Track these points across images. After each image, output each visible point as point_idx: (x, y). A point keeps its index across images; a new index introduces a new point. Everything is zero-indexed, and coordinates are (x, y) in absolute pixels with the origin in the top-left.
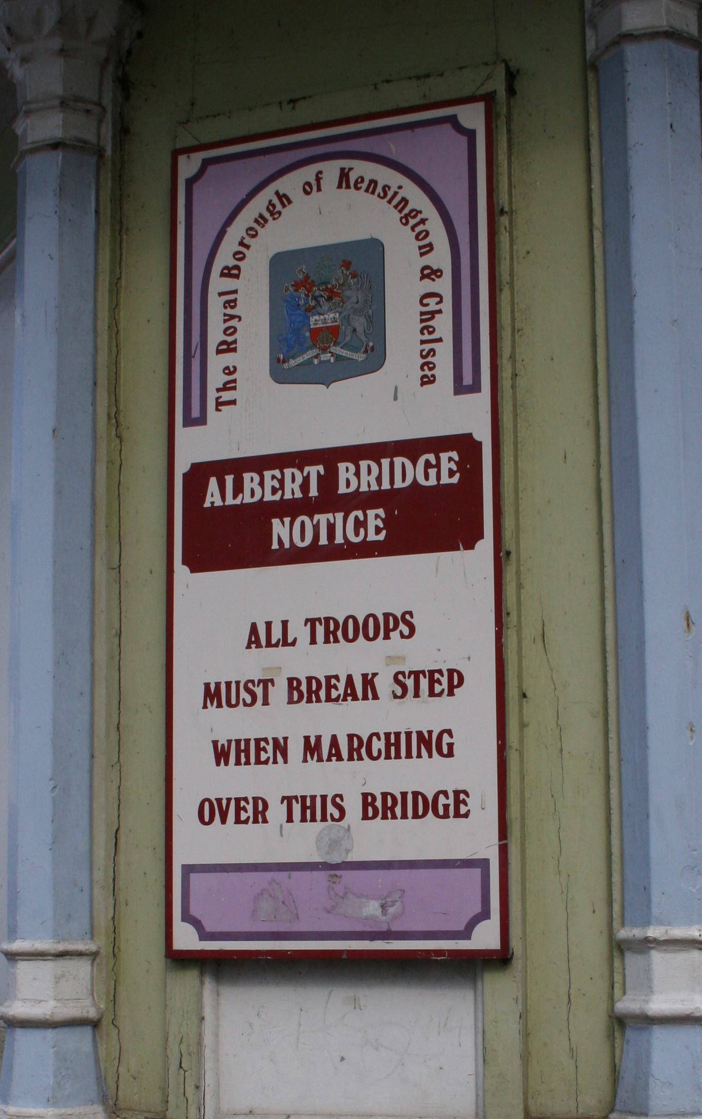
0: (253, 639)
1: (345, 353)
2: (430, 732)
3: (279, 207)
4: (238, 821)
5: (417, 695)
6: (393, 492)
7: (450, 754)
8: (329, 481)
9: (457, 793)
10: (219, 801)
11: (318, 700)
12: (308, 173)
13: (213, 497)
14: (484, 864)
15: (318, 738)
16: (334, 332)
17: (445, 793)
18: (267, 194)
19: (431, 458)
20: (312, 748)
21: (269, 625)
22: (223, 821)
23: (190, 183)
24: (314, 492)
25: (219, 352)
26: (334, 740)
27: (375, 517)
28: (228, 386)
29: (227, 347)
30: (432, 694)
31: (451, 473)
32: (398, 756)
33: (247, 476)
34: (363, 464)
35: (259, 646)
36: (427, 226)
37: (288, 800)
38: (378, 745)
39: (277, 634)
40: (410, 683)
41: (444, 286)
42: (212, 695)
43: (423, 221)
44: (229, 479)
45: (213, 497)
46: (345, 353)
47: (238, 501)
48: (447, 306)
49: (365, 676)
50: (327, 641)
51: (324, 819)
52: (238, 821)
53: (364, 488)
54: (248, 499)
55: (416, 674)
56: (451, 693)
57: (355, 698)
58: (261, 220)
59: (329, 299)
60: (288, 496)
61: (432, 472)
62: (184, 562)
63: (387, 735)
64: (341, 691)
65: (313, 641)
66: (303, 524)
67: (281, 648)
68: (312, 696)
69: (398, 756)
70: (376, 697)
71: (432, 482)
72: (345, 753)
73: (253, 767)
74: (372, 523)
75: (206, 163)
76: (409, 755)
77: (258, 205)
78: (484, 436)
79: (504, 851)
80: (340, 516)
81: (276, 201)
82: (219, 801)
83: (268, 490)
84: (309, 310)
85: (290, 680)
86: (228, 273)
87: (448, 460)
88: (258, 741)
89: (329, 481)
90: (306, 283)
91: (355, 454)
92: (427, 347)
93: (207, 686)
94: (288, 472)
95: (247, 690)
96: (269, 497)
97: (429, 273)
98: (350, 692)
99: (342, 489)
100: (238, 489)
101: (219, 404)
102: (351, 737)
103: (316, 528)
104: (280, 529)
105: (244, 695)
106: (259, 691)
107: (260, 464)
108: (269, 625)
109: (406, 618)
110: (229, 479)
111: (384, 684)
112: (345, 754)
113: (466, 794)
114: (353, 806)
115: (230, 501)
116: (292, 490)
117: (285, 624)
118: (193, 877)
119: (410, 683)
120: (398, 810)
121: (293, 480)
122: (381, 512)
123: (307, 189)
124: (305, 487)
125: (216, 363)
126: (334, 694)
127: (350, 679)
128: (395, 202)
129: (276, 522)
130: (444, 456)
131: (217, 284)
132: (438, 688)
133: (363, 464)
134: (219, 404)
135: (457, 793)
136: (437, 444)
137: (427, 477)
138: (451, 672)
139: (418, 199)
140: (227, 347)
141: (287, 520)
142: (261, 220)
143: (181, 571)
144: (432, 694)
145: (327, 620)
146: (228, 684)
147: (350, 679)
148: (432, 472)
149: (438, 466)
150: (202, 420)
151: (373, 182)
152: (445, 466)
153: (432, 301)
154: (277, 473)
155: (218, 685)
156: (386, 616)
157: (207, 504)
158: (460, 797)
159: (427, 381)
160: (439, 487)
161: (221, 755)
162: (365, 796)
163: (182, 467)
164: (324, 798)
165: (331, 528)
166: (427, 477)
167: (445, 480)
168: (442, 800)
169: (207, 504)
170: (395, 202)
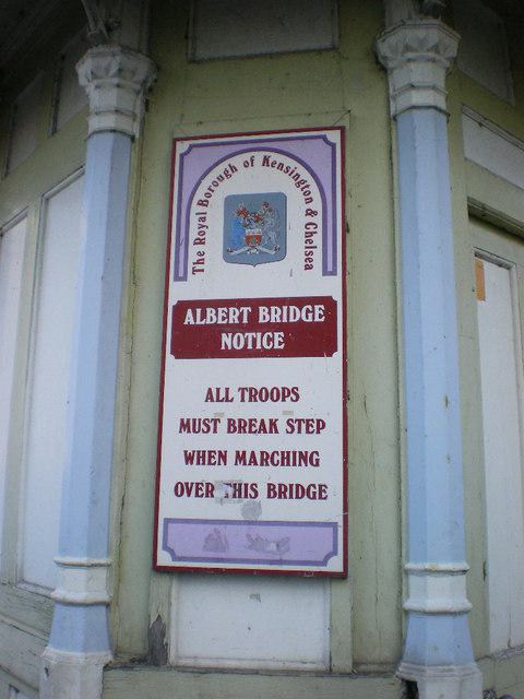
0: (209, 397)
1: (265, 250)
2: (306, 452)
3: (230, 172)
4: (197, 495)
5: (299, 432)
6: (288, 323)
7: (317, 465)
8: (254, 316)
9: (320, 486)
10: (187, 484)
11: (245, 432)
12: (247, 156)
13: (189, 319)
14: (334, 525)
15: (244, 453)
16: (259, 238)
17: (314, 486)
18: (224, 165)
19: (310, 307)
20: (240, 457)
21: (218, 390)
22: (189, 495)
23: (182, 156)
24: (245, 321)
25: (195, 244)
26: (253, 454)
27: (278, 336)
29: (201, 242)
30: (308, 432)
31: (320, 316)
32: (288, 464)
33: (209, 310)
34: (273, 308)
35: (212, 401)
36: (310, 189)
38: (278, 458)
39: (222, 395)
40: (296, 425)
41: (318, 220)
42: (185, 425)
43: (307, 186)
44: (199, 311)
45: (189, 319)
46: (265, 250)
47: (203, 323)
48: (320, 230)
49: (271, 420)
50: (250, 401)
51: (246, 496)
52: (197, 495)
53: (273, 321)
54: (208, 322)
55: (300, 421)
56: (318, 432)
57: (265, 432)
58: (221, 178)
59: (256, 221)
60: (231, 322)
61: (310, 315)
63: (283, 453)
64: (258, 427)
65: (243, 400)
66: (239, 338)
67: (224, 403)
68: (242, 429)
69: (288, 464)
70: (277, 432)
71: (310, 320)
72: (259, 462)
73: (206, 467)
74: (277, 339)
75: (191, 147)
76: (294, 464)
77: (219, 170)
78: (338, 298)
79: (346, 519)
80: (259, 334)
81: (228, 168)
82: (187, 484)
83: (220, 318)
84: (246, 226)
85: (230, 420)
86: (201, 203)
88: (210, 452)
89: (254, 316)
90: (243, 212)
91: (269, 302)
92: (309, 250)
93: (182, 420)
94: (231, 309)
95: (204, 423)
96: (220, 322)
97: (310, 213)
98: (263, 429)
99: (261, 320)
100: (204, 316)
101: (194, 271)
102: (262, 453)
103: (246, 340)
104: (226, 339)
105: (202, 426)
106: (212, 425)
107: (216, 304)
108: (218, 390)
109: (294, 391)
110: (199, 311)
111: (282, 426)
112: (259, 462)
113: (325, 486)
114: (263, 490)
115: (198, 322)
116: (233, 319)
117: (227, 390)
118: (170, 525)
119: (296, 425)
120: (288, 494)
121: (234, 314)
122: (282, 334)
123: (246, 165)
124: (241, 318)
125: (193, 250)
126: (254, 429)
127: (263, 421)
128: (294, 174)
129: (224, 335)
130: (317, 307)
131: (195, 208)
132: (311, 429)
133: (273, 308)
134: (194, 271)
135: (320, 486)
136: (314, 301)
137: (307, 317)
138: (318, 421)
139: (305, 175)
140: (201, 242)
141: (230, 335)
142: (221, 178)
143: (170, 358)
144: (308, 432)
145: (251, 389)
146: (194, 420)
147: (263, 421)
148: (310, 315)
149: (313, 312)
150: (185, 278)
151: (281, 165)
152: (317, 312)
153: (312, 227)
154: (225, 309)
155: (188, 420)
156: (283, 389)
157: (186, 323)
158: (322, 488)
159: (308, 267)
160: (313, 323)
161: (189, 459)
162: (269, 485)
163: (172, 302)
164: (246, 485)
165: (254, 341)
166: (307, 317)
167: (317, 319)
168: (312, 489)
169: (186, 323)
170: (294, 174)
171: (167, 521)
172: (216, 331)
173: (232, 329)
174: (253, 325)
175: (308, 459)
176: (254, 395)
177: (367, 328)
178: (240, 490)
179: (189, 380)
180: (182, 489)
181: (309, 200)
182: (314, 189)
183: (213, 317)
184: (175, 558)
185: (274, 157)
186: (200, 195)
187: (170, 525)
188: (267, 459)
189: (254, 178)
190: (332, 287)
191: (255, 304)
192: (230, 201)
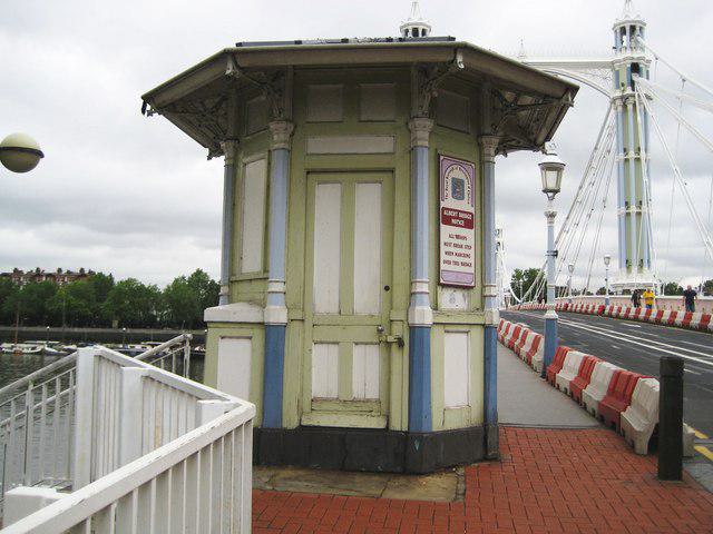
107: (452, 210)
173: (454, 218)
174: (457, 218)
175: (468, 256)
176: (458, 237)
177: (477, 223)
178: (456, 263)
180: (445, 262)
183: (450, 213)
188: (460, 255)
189: (458, 174)
190: (472, 210)
191: (459, 211)
192: (453, 179)
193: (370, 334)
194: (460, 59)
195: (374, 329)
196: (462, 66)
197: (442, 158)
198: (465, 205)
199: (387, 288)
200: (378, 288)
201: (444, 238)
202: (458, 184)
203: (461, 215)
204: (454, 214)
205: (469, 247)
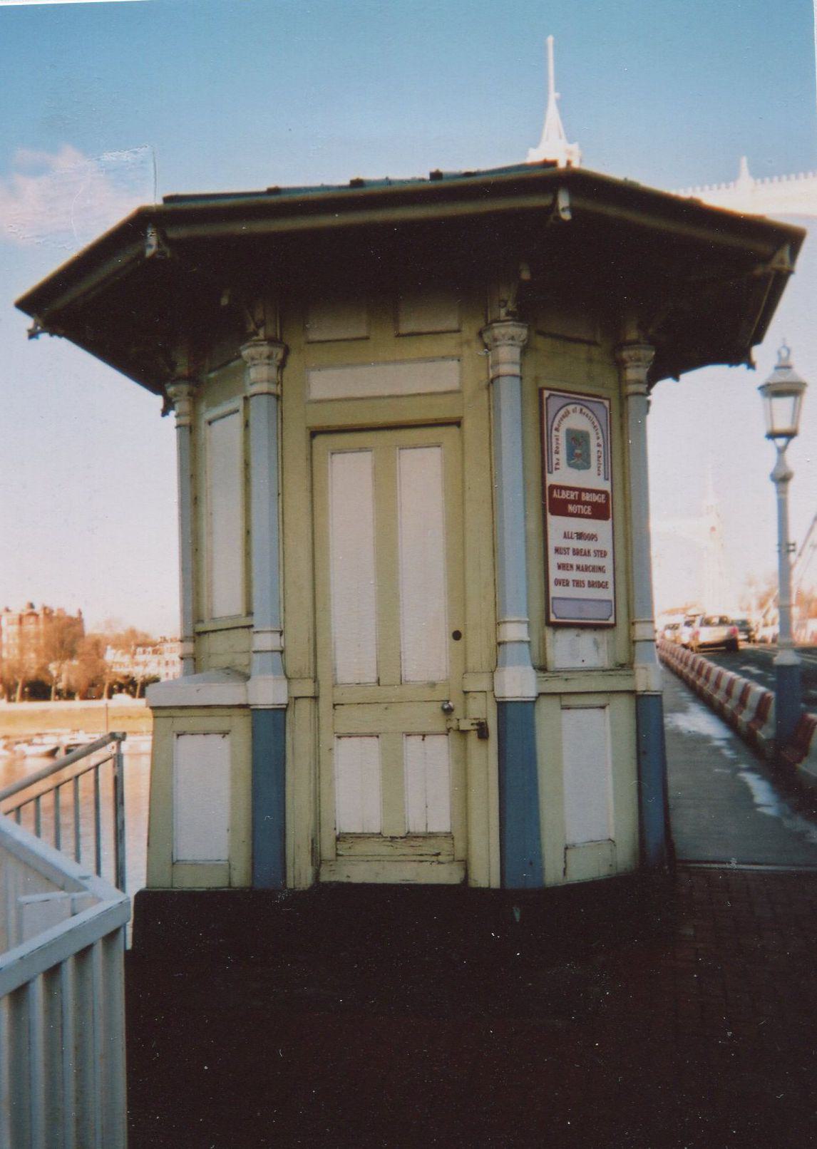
13: (555, 495)
20: (578, 568)
24: (577, 498)
27: (589, 508)
28: (557, 464)
37: (573, 581)
38: (591, 568)
39: (570, 536)
42: (557, 550)
45: (555, 495)
48: (602, 455)
62: (550, 511)
77: (562, 412)
79: (615, 598)
87: (603, 496)
89: (580, 496)
94: (571, 492)
98: (585, 554)
100: (560, 495)
101: (556, 469)
110: (559, 490)
114: (586, 583)
115: (559, 497)
116: (572, 497)
131: (554, 433)
139: (596, 423)
140: (557, 453)
143: (549, 515)
161: (559, 567)
163: (548, 484)
171: (554, 598)
172: (567, 502)
174: (578, 502)
175: (601, 569)
176: (580, 536)
178: (578, 584)
179: (557, 524)
180: (558, 582)
181: (598, 438)
182: (599, 431)
183: (565, 495)
184: (557, 618)
185: (585, 410)
186: (555, 425)
187: (555, 602)
189: (577, 420)
190: (606, 486)
191: (581, 490)
193: (430, 717)
194: (564, 201)
195: (436, 708)
196: (566, 216)
197: (546, 393)
198: (592, 479)
199: (457, 635)
200: (444, 636)
201: (555, 540)
202: (577, 441)
203: (586, 497)
204: (573, 495)
205: (602, 554)
